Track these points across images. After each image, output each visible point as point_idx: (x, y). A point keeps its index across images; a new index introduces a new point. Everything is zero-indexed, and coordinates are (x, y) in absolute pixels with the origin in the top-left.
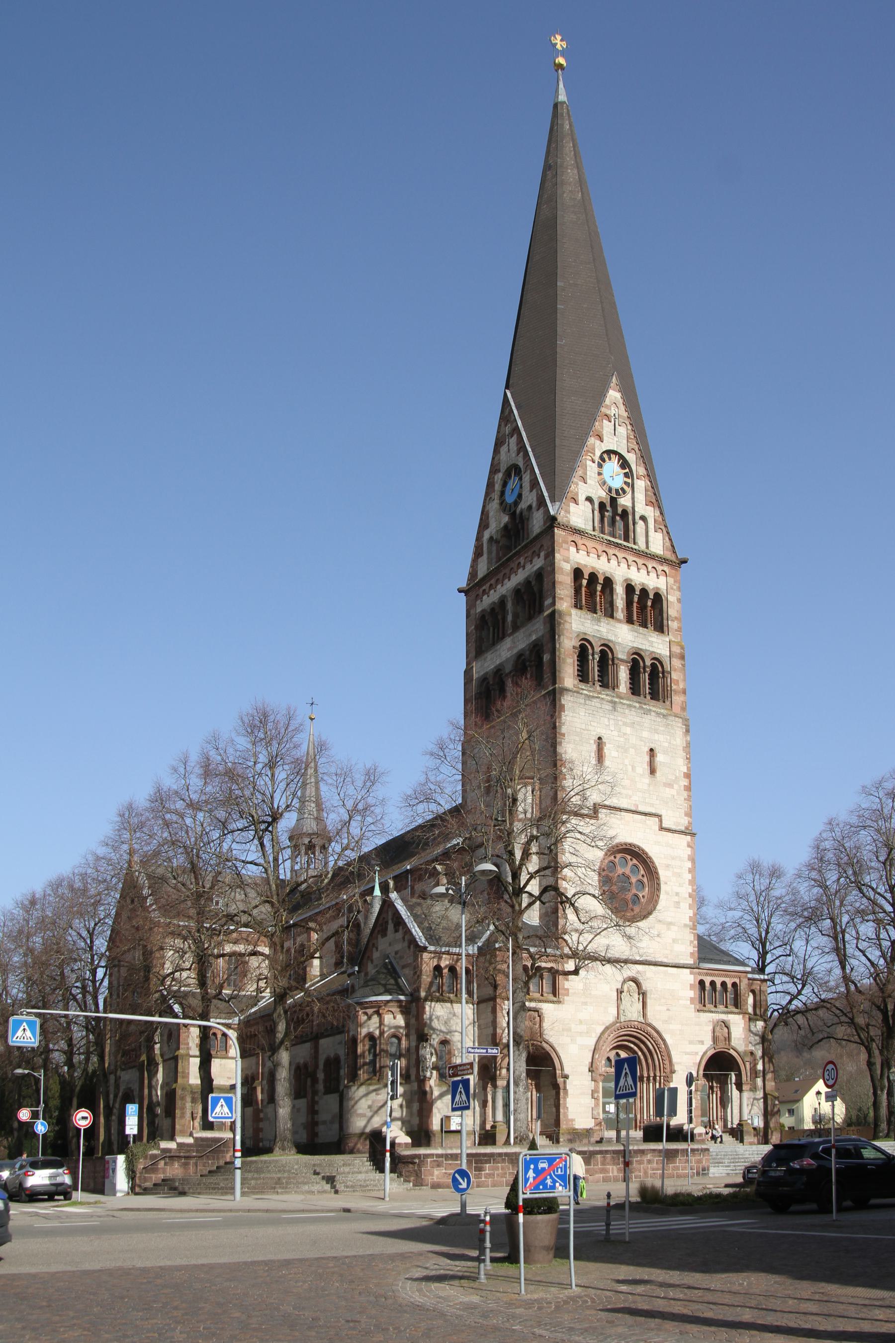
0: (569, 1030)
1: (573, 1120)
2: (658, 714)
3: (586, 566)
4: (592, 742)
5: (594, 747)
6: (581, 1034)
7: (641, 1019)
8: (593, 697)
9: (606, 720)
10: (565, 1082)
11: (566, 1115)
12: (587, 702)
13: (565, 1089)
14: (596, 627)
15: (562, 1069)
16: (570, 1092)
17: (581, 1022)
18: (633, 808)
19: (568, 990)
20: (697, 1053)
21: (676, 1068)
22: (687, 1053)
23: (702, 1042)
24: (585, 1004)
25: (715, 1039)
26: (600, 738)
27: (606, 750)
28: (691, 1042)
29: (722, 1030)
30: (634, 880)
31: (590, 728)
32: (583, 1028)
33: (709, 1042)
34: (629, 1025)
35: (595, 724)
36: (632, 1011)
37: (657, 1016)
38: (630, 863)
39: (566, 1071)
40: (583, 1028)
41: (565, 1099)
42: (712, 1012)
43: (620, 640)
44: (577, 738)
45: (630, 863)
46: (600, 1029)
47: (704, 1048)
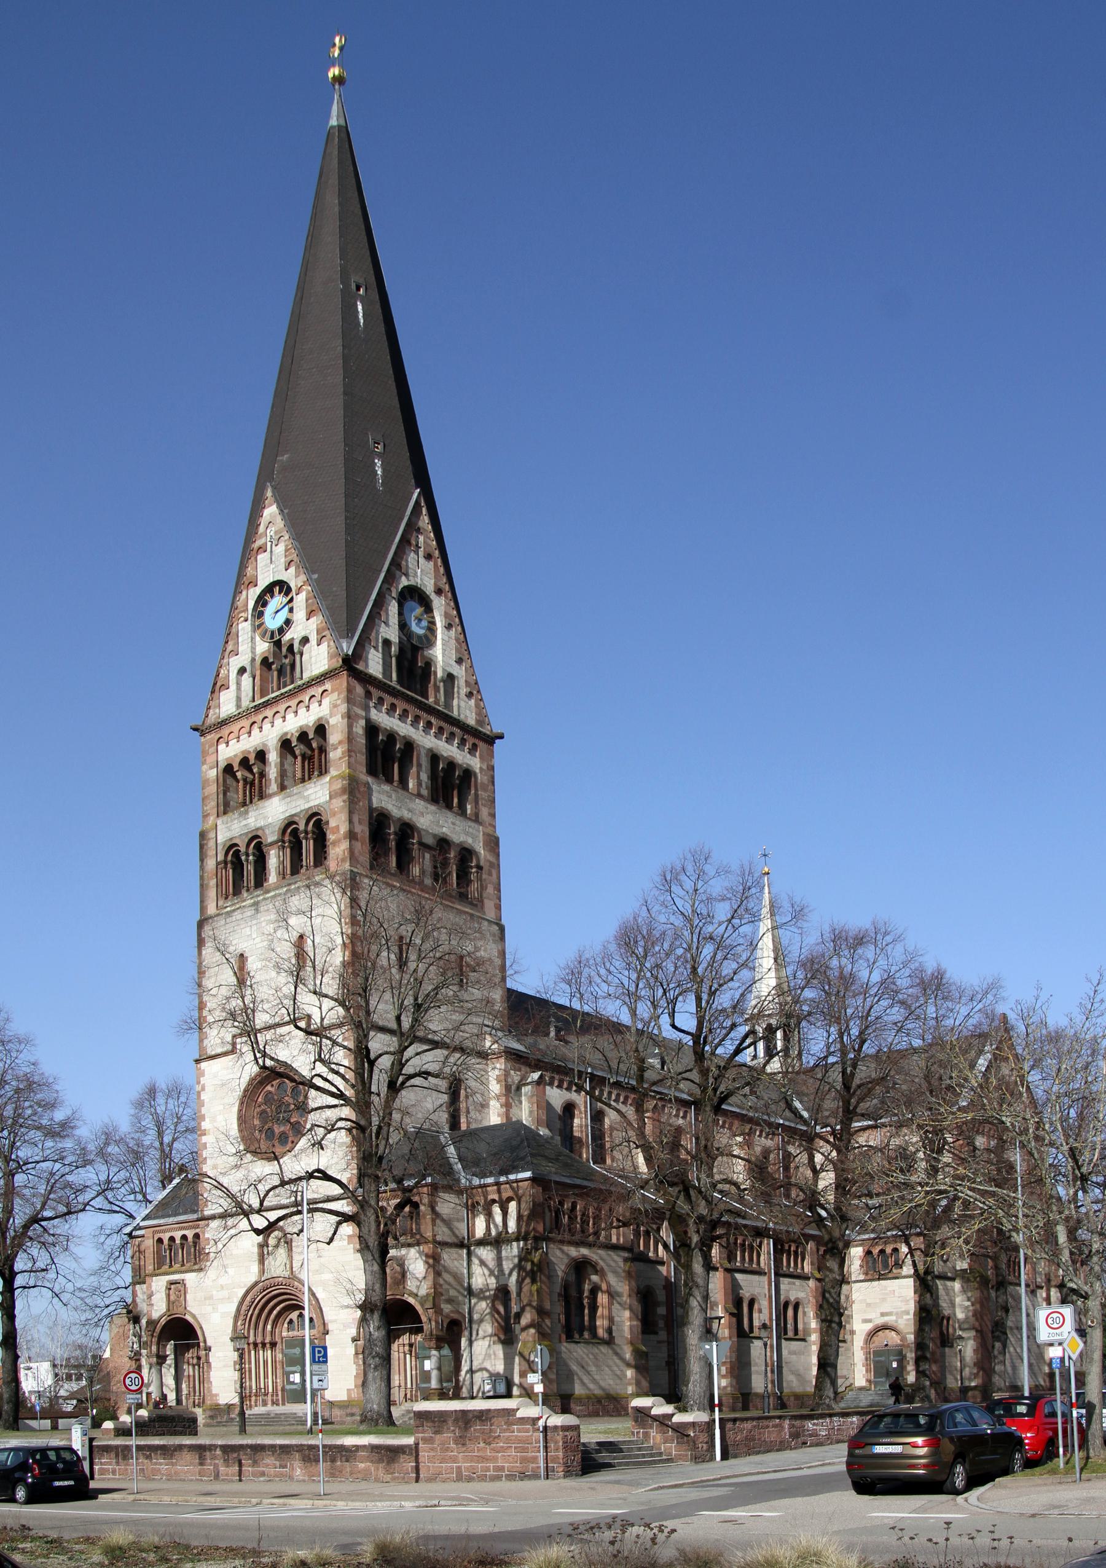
0: (211, 1298)
1: (217, 1395)
3: (235, 756)
8: (234, 911)
9: (248, 929)
10: (207, 1355)
11: (210, 1390)
13: (208, 1362)
14: (244, 822)
15: (205, 1341)
16: (213, 1365)
17: (222, 1287)
21: (330, 1327)
32: (225, 1293)
36: (277, 1265)
39: (209, 1344)
40: (225, 1293)
41: (209, 1372)
43: (270, 820)
46: (241, 1292)
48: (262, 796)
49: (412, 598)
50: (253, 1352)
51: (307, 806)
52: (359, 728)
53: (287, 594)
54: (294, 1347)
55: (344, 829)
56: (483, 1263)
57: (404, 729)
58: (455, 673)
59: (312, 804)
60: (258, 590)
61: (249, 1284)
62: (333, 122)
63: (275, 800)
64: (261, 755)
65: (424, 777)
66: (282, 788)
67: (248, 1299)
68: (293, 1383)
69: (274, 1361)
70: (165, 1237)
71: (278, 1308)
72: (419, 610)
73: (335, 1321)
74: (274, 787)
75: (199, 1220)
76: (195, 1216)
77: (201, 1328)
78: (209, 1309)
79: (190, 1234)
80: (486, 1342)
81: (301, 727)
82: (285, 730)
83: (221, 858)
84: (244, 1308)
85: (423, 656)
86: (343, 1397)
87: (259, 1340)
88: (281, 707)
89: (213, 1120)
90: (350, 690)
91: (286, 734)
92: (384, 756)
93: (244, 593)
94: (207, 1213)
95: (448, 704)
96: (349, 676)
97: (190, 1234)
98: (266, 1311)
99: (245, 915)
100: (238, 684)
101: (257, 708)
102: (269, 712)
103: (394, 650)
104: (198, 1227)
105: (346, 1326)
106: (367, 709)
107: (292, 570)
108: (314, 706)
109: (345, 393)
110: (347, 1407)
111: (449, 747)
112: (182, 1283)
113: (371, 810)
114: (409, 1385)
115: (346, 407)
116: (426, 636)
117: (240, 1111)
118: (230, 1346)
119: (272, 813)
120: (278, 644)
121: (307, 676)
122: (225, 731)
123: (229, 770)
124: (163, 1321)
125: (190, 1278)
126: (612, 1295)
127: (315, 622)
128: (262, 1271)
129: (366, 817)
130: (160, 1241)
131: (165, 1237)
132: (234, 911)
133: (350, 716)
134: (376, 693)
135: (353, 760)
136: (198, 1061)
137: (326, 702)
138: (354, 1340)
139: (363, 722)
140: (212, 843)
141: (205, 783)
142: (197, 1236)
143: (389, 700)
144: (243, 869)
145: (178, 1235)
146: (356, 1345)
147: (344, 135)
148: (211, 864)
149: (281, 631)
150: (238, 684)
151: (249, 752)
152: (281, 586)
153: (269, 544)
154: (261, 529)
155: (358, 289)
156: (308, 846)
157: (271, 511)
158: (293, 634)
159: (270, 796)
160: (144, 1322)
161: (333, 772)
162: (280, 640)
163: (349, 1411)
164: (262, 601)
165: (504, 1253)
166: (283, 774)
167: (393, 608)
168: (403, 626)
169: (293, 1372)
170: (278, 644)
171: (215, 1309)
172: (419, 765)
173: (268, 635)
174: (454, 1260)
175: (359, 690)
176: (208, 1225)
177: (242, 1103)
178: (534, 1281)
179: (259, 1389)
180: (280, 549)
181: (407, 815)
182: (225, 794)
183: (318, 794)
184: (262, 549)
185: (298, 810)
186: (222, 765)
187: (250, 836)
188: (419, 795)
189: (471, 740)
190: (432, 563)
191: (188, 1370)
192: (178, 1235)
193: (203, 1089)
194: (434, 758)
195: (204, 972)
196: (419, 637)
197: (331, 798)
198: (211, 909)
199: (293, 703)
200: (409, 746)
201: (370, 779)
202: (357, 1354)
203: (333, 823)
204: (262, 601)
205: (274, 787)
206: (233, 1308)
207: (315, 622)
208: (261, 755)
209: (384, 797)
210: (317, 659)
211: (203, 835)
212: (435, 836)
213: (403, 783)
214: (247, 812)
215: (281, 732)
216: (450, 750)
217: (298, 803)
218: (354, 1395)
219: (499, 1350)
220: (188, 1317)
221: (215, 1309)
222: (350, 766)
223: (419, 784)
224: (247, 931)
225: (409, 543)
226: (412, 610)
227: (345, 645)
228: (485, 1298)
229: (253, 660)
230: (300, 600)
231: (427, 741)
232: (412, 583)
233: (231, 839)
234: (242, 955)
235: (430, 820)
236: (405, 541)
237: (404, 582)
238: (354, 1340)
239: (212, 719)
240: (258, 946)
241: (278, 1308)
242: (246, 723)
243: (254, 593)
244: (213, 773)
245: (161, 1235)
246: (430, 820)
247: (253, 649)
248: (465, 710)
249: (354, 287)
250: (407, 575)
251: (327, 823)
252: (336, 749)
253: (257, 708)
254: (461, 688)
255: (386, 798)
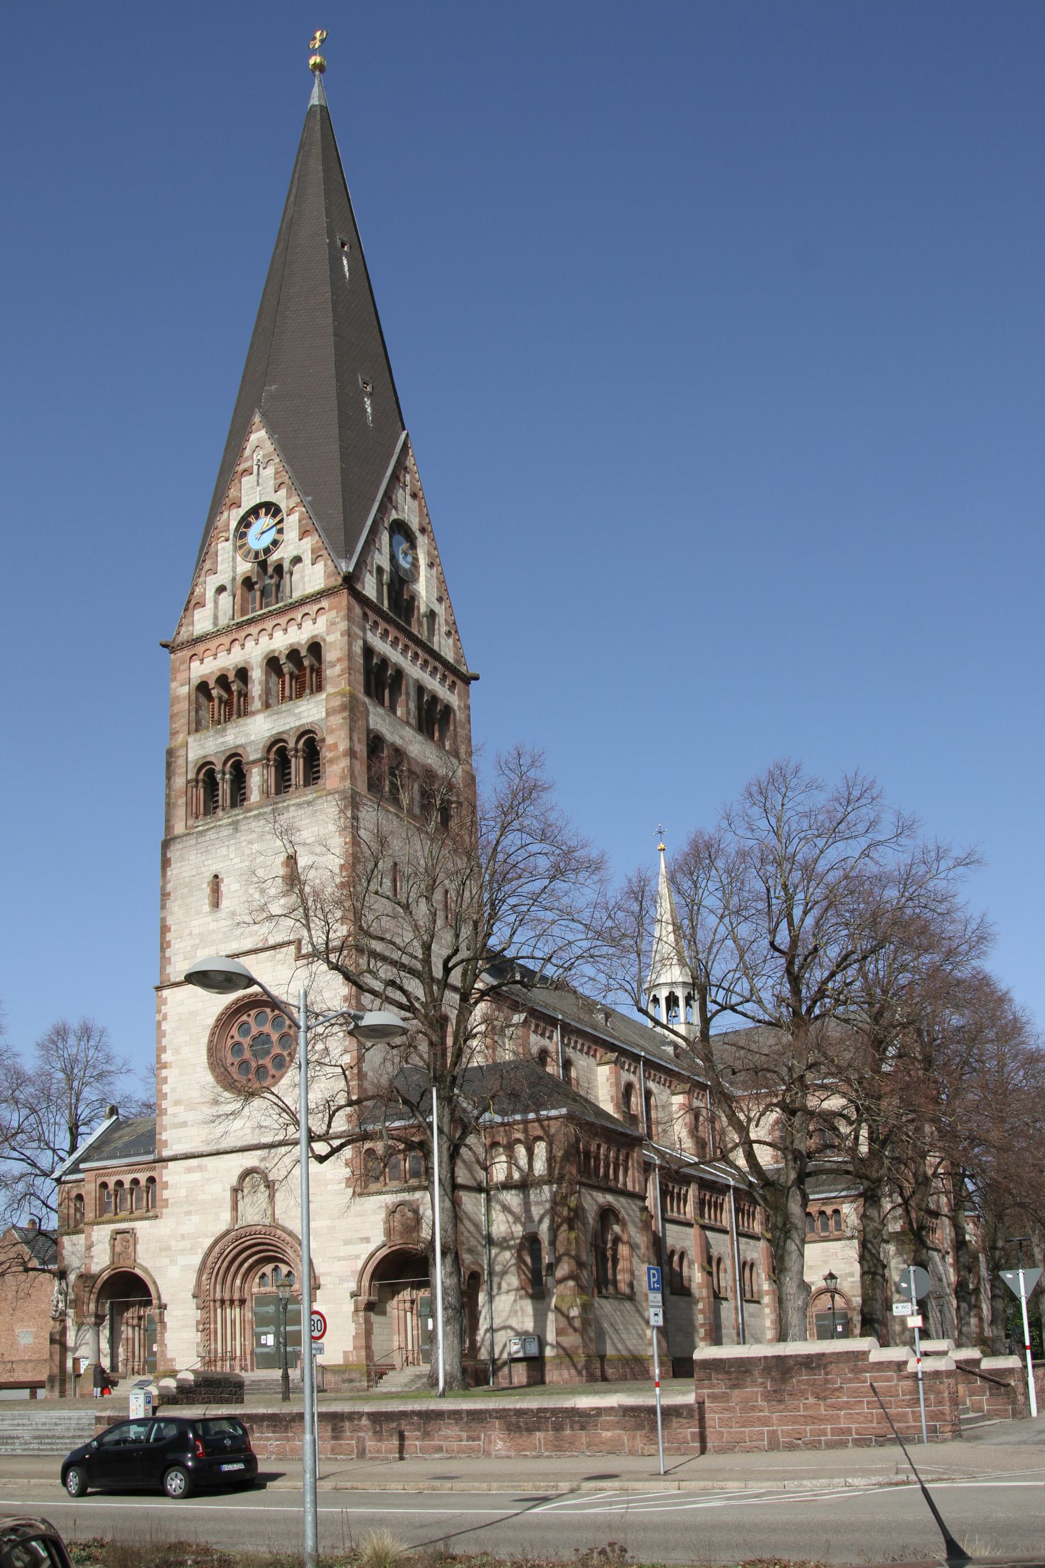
0: (168, 1249)
1: (172, 1360)
2: (299, 805)
3: (212, 673)
4: (205, 885)
5: (207, 890)
6: (183, 1252)
7: (267, 1222)
8: (208, 830)
9: (224, 849)
10: (161, 1314)
12: (200, 840)
13: (162, 1322)
14: (221, 740)
15: (159, 1298)
17: (183, 1237)
18: (260, 945)
19: (167, 1200)
20: (358, 1257)
21: (322, 1281)
22: (340, 1259)
23: (367, 1240)
24: (189, 1213)
25: (389, 1232)
26: (216, 876)
27: (223, 888)
28: (347, 1242)
29: (405, 1219)
30: (275, 1037)
31: (203, 869)
32: (187, 1244)
33: (378, 1238)
34: (248, 1231)
35: (210, 862)
37: (288, 1213)
38: (251, 1020)
39: (164, 1300)
40: (187, 1244)
41: (162, 1333)
42: (381, 1193)
43: (253, 738)
44: (186, 890)
45: (251, 1020)
46: (208, 1242)
47: (372, 1247)
48: (244, 713)
49: (399, 533)
50: (219, 1311)
51: (297, 724)
52: (358, 648)
53: (274, 516)
54: (267, 1304)
55: (343, 746)
56: (506, 1209)
57: (395, 656)
58: (436, 611)
59: (304, 721)
60: (242, 511)
61: (218, 1234)
62: (315, 101)
63: (260, 718)
64: (243, 674)
65: (412, 706)
66: (267, 706)
67: (217, 1249)
68: (265, 1345)
69: (243, 1321)
70: (111, 1182)
71: (250, 1261)
72: (405, 545)
73: (329, 1274)
74: (257, 704)
75: (155, 1161)
76: (151, 1157)
77: (155, 1283)
78: (167, 1261)
79: (143, 1177)
80: (511, 1297)
81: (291, 645)
82: (272, 647)
83: (191, 775)
84: (211, 1259)
85: (409, 590)
86: (339, 1360)
87: (227, 1297)
88: (269, 624)
89: (177, 1051)
90: (350, 609)
91: (274, 651)
92: (378, 679)
93: (226, 514)
94: (166, 1153)
95: (431, 640)
96: (349, 594)
97: (143, 1177)
98: (236, 1263)
99: (221, 835)
100: (216, 602)
101: (240, 626)
102: (253, 630)
103: (386, 578)
104: (154, 1169)
105: (342, 1280)
106: (364, 630)
107: (283, 492)
108: (307, 624)
109: (335, 335)
110: (343, 1372)
111: (432, 680)
112: (131, 1232)
113: (369, 731)
114: (410, 1347)
115: (336, 347)
116: (411, 570)
117: (211, 1042)
118: (192, 1303)
119: (255, 731)
120: (263, 565)
121: (297, 595)
122: (200, 648)
123: (203, 688)
124: (105, 1276)
125: (141, 1227)
126: (633, 1247)
127: (308, 543)
128: (235, 1219)
129: (364, 737)
130: (104, 1185)
131: (111, 1182)
132: (208, 830)
133: (349, 634)
134: (373, 617)
135: (352, 678)
136: (159, 989)
137: (322, 620)
138: (354, 1295)
139: (360, 643)
140: (181, 761)
141: (175, 700)
142: (152, 1180)
143: (383, 625)
144: (220, 788)
145: (127, 1179)
146: (356, 1302)
147: (324, 114)
148: (180, 782)
149: (267, 551)
150: (216, 602)
151: (229, 670)
152: (271, 508)
153: (255, 468)
154: (247, 452)
155: (343, 246)
156: (297, 767)
157: (259, 436)
158: (282, 554)
159: (253, 713)
160: (72, 1277)
161: (330, 689)
162: (265, 561)
163: (346, 1376)
164: (245, 523)
165: (532, 1197)
166: (267, 692)
167: (385, 537)
168: (393, 558)
169: (266, 1334)
170: (263, 565)
171: (173, 1262)
172: (408, 694)
173: (252, 555)
174: (472, 1203)
175: (358, 610)
176: (166, 1167)
177: (213, 1034)
178: (571, 1228)
179: (224, 1352)
180: (270, 471)
181: (399, 742)
182: (197, 712)
183: (310, 711)
184: (248, 472)
185: (287, 727)
186: (195, 682)
187: (228, 754)
188: (408, 723)
189: (451, 678)
190: (417, 502)
191: (126, 1332)
192: (127, 1179)
193: (165, 1018)
194: (421, 689)
195: (169, 894)
196: (405, 570)
197: (328, 714)
198: (179, 828)
199: (283, 620)
200: (399, 673)
201: (367, 700)
202: (356, 1311)
203: (330, 740)
204: (245, 523)
205: (257, 704)
206: (197, 1260)
207: (308, 543)
208: (243, 674)
209: (378, 720)
210: (311, 577)
211: (170, 753)
212: (423, 766)
213: (393, 709)
214: (224, 730)
215: (267, 650)
216: (434, 684)
217: (287, 720)
218: (353, 1358)
219: (528, 1305)
220: (137, 1271)
221: (173, 1262)
222: (350, 684)
223: (408, 713)
224: (224, 851)
225: (398, 480)
226: (400, 544)
227: (343, 565)
228: (509, 1248)
229: (234, 579)
230: (292, 523)
231: (414, 671)
232: (401, 517)
233: (205, 757)
234: (216, 876)
235: (419, 749)
236: (395, 478)
237: (394, 515)
238: (354, 1295)
239: (184, 635)
240: (236, 867)
241: (250, 1261)
242: (226, 640)
243: (234, 517)
244: (185, 690)
245: (105, 1179)
246: (419, 749)
247: (234, 568)
248: (446, 648)
249: (339, 243)
250: (396, 508)
251: (323, 740)
252: (335, 666)
253: (240, 626)
254: (441, 627)
255: (381, 722)
